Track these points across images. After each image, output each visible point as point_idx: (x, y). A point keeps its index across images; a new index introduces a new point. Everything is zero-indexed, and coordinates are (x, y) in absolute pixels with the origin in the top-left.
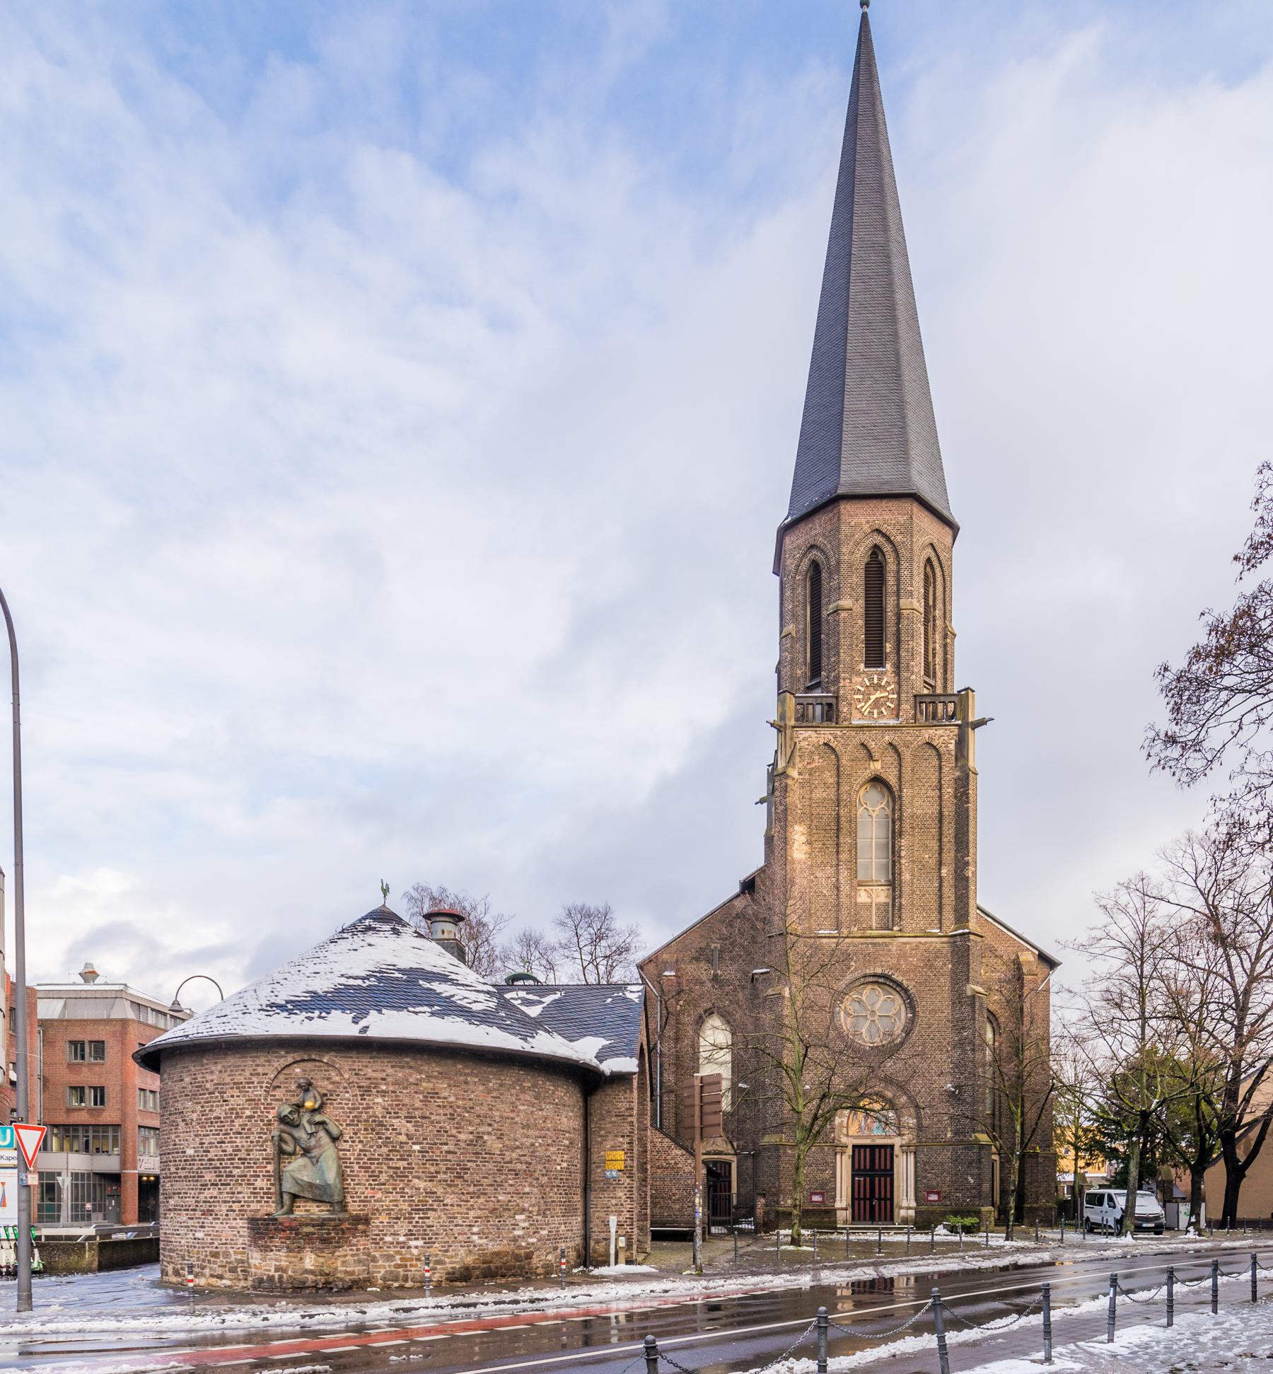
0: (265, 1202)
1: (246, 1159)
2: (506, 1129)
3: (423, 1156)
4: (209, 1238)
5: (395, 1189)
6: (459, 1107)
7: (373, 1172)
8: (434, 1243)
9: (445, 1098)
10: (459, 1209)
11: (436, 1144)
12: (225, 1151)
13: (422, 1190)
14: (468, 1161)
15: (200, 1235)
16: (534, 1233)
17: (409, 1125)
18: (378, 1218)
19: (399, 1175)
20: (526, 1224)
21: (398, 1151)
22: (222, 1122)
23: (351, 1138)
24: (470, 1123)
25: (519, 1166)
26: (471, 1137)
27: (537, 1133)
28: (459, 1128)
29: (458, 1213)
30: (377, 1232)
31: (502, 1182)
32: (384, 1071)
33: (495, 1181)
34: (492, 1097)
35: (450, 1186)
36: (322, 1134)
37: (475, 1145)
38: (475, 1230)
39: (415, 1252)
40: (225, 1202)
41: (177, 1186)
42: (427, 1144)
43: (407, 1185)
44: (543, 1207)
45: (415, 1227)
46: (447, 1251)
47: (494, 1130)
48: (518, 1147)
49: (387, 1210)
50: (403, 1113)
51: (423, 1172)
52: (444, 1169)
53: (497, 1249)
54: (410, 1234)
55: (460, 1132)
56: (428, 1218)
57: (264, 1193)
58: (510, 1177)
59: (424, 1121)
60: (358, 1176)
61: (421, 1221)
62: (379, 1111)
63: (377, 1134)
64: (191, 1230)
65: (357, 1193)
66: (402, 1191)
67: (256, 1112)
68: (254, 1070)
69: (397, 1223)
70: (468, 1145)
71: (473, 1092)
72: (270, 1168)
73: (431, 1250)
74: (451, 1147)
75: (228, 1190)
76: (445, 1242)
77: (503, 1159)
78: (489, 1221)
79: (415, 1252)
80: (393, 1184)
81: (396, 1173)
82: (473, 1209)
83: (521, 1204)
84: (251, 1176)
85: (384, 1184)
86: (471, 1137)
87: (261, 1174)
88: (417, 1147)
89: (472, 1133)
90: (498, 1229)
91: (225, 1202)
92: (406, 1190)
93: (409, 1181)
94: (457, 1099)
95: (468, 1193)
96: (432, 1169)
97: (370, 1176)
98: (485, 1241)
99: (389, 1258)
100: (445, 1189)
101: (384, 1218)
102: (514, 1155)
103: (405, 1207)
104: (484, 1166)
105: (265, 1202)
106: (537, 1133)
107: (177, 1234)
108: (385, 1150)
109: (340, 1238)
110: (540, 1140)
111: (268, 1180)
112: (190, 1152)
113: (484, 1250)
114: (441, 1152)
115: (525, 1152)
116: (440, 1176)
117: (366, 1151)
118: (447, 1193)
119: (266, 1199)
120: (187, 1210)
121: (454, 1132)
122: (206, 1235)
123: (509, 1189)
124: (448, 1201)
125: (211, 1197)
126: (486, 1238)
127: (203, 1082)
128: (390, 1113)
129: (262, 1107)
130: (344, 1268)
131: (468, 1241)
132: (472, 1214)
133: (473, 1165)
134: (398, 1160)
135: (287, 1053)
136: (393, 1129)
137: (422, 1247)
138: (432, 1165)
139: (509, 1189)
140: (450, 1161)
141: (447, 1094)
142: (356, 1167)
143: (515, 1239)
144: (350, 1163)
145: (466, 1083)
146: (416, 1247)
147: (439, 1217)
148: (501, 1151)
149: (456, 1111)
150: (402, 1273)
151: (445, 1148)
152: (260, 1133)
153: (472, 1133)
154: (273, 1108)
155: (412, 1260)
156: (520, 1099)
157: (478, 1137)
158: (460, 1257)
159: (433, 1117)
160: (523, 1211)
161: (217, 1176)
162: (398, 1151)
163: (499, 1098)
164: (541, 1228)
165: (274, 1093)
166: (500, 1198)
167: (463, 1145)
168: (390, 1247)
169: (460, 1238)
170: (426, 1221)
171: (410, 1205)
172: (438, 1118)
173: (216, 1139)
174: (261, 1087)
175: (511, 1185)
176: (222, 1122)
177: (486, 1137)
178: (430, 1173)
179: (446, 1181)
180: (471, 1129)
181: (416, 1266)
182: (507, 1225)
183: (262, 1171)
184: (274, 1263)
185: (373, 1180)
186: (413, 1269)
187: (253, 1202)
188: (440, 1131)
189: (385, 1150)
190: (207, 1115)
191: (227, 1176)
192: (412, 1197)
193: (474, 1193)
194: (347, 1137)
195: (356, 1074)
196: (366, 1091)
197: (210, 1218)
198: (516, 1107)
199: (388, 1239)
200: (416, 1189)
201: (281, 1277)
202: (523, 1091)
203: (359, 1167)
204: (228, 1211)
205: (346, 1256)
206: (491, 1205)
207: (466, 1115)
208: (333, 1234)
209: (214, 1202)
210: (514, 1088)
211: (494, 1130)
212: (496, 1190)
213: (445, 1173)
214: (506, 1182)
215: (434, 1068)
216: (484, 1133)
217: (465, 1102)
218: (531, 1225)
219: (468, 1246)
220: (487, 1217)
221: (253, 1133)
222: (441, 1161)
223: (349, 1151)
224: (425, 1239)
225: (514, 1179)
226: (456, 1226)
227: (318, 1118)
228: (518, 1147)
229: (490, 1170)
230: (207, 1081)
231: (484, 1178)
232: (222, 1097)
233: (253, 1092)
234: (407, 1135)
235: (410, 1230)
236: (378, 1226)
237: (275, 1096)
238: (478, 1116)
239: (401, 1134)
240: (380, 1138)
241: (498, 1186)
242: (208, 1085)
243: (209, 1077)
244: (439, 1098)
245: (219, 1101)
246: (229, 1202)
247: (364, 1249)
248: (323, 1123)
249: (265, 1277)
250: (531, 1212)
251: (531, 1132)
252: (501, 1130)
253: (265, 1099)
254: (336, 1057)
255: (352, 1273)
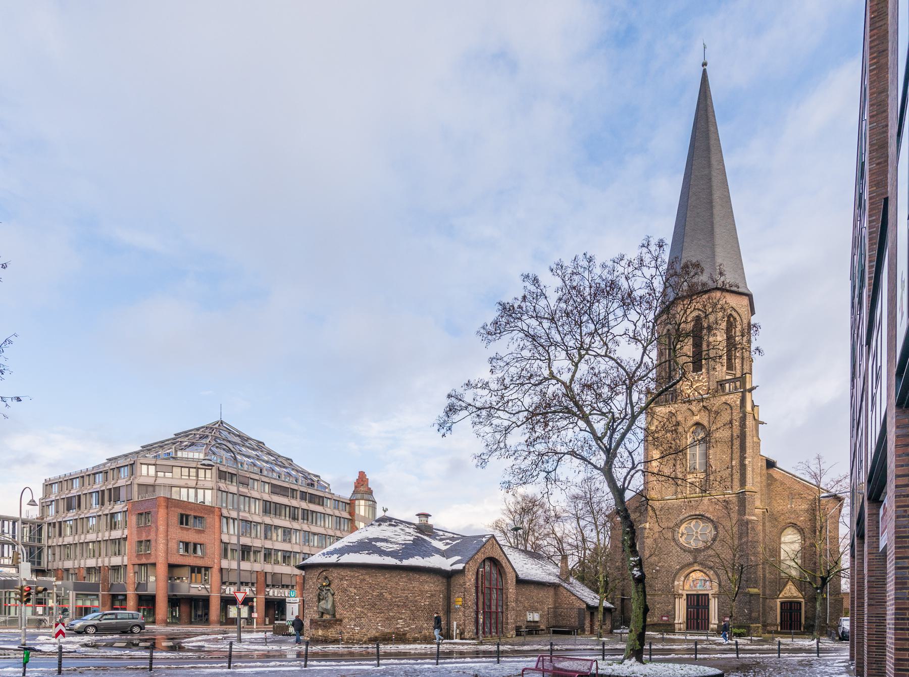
2: (393, 591)
19: (351, 606)
24: (378, 589)
25: (399, 603)
27: (409, 592)
39: (357, 631)
44: (412, 617)
50: (353, 586)
53: (389, 631)
54: (355, 625)
62: (345, 586)
66: (353, 612)
74: (370, 597)
88: (357, 597)
96: (363, 604)
99: (348, 633)
101: (347, 620)
103: (354, 616)
106: (409, 592)
108: (347, 598)
124: (369, 615)
131: (377, 628)
132: (378, 619)
143: (398, 628)
145: (376, 576)
158: (373, 633)
160: (401, 619)
189: (347, 598)
196: (341, 579)
199: (348, 627)
202: (402, 578)
215: (364, 572)
255: (335, 637)
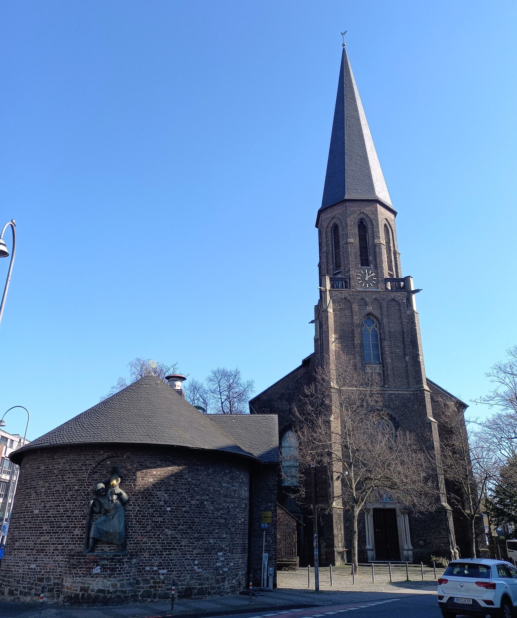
0: (78, 544)
1: (71, 516)
3: (172, 514)
4: (39, 568)
5: (154, 535)
6: (193, 484)
7: (144, 524)
8: (173, 571)
9: (186, 479)
11: (179, 507)
12: (59, 511)
13: (169, 536)
14: (196, 518)
15: (33, 566)
16: (227, 564)
17: (166, 495)
18: (143, 555)
21: (159, 511)
22: (60, 493)
23: (133, 503)
24: (198, 494)
28: (192, 497)
29: (188, 551)
30: (142, 564)
31: (212, 531)
32: (156, 463)
33: (209, 530)
34: (210, 478)
35: (185, 533)
37: (200, 508)
38: (196, 562)
39: (162, 577)
40: (54, 544)
41: (23, 534)
42: (175, 507)
43: (161, 533)
45: (163, 560)
46: (180, 577)
47: (210, 498)
49: (149, 549)
51: (171, 525)
54: (160, 566)
55: (192, 500)
56: (171, 554)
57: (78, 538)
58: (216, 527)
59: (174, 492)
60: (134, 527)
61: (167, 556)
63: (148, 500)
64: (28, 563)
65: (132, 538)
67: (81, 488)
68: (84, 462)
69: (153, 558)
70: (196, 507)
71: (201, 475)
72: (84, 522)
73: (171, 576)
74: (187, 509)
75: (56, 536)
76: (179, 571)
77: (213, 516)
78: (204, 557)
79: (162, 577)
80: (153, 533)
81: (156, 525)
82: (196, 549)
84: (72, 527)
85: (149, 532)
87: (78, 526)
89: (198, 500)
90: (208, 562)
91: (54, 544)
92: (161, 536)
93: (163, 530)
94: (192, 479)
95: (194, 538)
96: (176, 522)
97: (141, 527)
98: (201, 570)
99: (146, 581)
100: (182, 535)
101: (146, 555)
102: (219, 514)
103: (159, 547)
104: (203, 520)
105: (78, 544)
107: (17, 566)
108: (151, 510)
109: (121, 568)
111: (82, 530)
112: (36, 512)
113: (200, 576)
114: (182, 512)
116: (180, 527)
117: (141, 511)
118: (183, 538)
119: (79, 542)
120: (28, 549)
122: (37, 566)
124: (183, 543)
125: (45, 541)
126: (202, 568)
127: (52, 469)
128: (156, 488)
129: (86, 484)
130: (121, 589)
132: (195, 552)
134: (158, 516)
135: (104, 452)
136: (157, 498)
137: (166, 574)
138: (176, 520)
140: (186, 517)
141: (187, 477)
142: (134, 521)
144: (131, 519)
146: (163, 574)
147: (177, 554)
148: (213, 511)
149: (191, 487)
150: (153, 592)
151: (184, 509)
152: (81, 500)
153: (198, 500)
154: (92, 485)
155: (159, 583)
156: (223, 480)
157: (201, 503)
161: (51, 527)
162: (159, 511)
163: (213, 479)
164: (230, 562)
165: (93, 476)
166: (210, 541)
167: (193, 507)
168: (148, 574)
169: (188, 568)
170: (170, 556)
171: (162, 546)
172: (181, 491)
173: (54, 504)
174: (87, 472)
175: (217, 533)
176: (60, 493)
177: (205, 503)
178: (175, 525)
179: (183, 530)
181: (161, 587)
182: (213, 559)
183: (79, 524)
184: (80, 585)
185: (143, 530)
186: (160, 589)
187: (71, 544)
188: (182, 499)
189: (151, 510)
190: (51, 489)
191: (58, 527)
192: (163, 540)
193: (197, 538)
195: (140, 465)
197: (42, 554)
198: (222, 484)
200: (166, 535)
201: (83, 595)
203: (136, 521)
204: (54, 550)
205: (123, 580)
207: (196, 489)
208: (118, 566)
209: (46, 544)
210: (221, 473)
211: (210, 498)
212: (209, 536)
213: (183, 525)
214: (214, 531)
216: (204, 500)
217: (196, 481)
218: (225, 559)
219: (192, 573)
220: (203, 554)
221: (77, 500)
222: (181, 517)
223: (131, 511)
224: (168, 568)
225: (218, 529)
226: (186, 559)
229: (206, 523)
230: (55, 469)
231: (203, 528)
232: (63, 478)
233: (82, 475)
234: (164, 501)
235: (160, 563)
236: (142, 560)
237: (94, 477)
239: (161, 501)
240: (150, 503)
241: (210, 533)
242: (55, 471)
243: (57, 466)
244: (183, 479)
245: (60, 481)
246: (56, 544)
247: (133, 575)
249: (73, 595)
250: (226, 551)
251: (228, 499)
252: (213, 498)
253: (88, 480)
254: (131, 455)
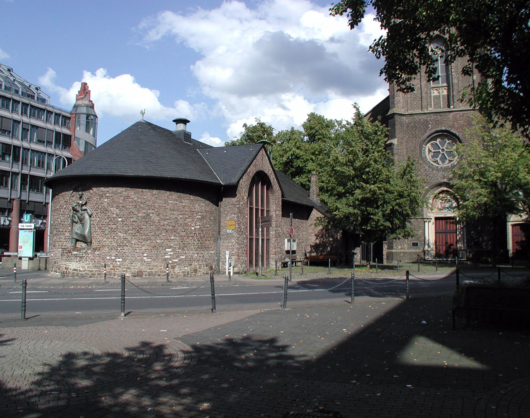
2: (161, 211)
10: (138, 246)
19: (113, 231)
20: (172, 253)
24: (144, 209)
25: (168, 227)
26: (144, 215)
27: (179, 213)
28: (139, 211)
35: (134, 236)
36: (86, 214)
38: (145, 255)
44: (182, 246)
48: (167, 219)
50: (115, 205)
52: (131, 228)
54: (116, 256)
74: (135, 219)
83: (169, 244)
86: (144, 215)
88: (120, 219)
96: (126, 229)
103: (115, 244)
106: (179, 213)
110: (181, 216)
115: (172, 221)
121: (136, 213)
123: (162, 237)
131: (142, 260)
132: (144, 248)
133: (145, 227)
139: (162, 237)
147: (129, 249)
159: (127, 207)
160: (170, 247)
167: (140, 218)
169: (138, 258)
177: (151, 215)
180: (144, 211)
189: (107, 220)
194: (94, 215)
206: (153, 244)
213: (132, 230)
216: (150, 213)
227: (84, 208)
228: (167, 219)
238: (148, 206)
248: (86, 210)
